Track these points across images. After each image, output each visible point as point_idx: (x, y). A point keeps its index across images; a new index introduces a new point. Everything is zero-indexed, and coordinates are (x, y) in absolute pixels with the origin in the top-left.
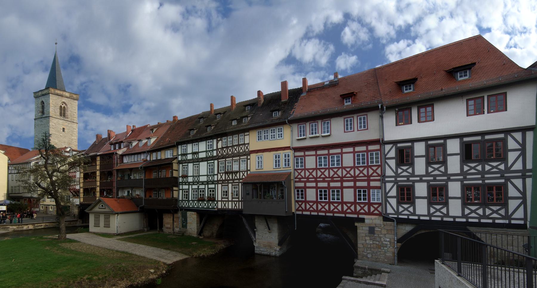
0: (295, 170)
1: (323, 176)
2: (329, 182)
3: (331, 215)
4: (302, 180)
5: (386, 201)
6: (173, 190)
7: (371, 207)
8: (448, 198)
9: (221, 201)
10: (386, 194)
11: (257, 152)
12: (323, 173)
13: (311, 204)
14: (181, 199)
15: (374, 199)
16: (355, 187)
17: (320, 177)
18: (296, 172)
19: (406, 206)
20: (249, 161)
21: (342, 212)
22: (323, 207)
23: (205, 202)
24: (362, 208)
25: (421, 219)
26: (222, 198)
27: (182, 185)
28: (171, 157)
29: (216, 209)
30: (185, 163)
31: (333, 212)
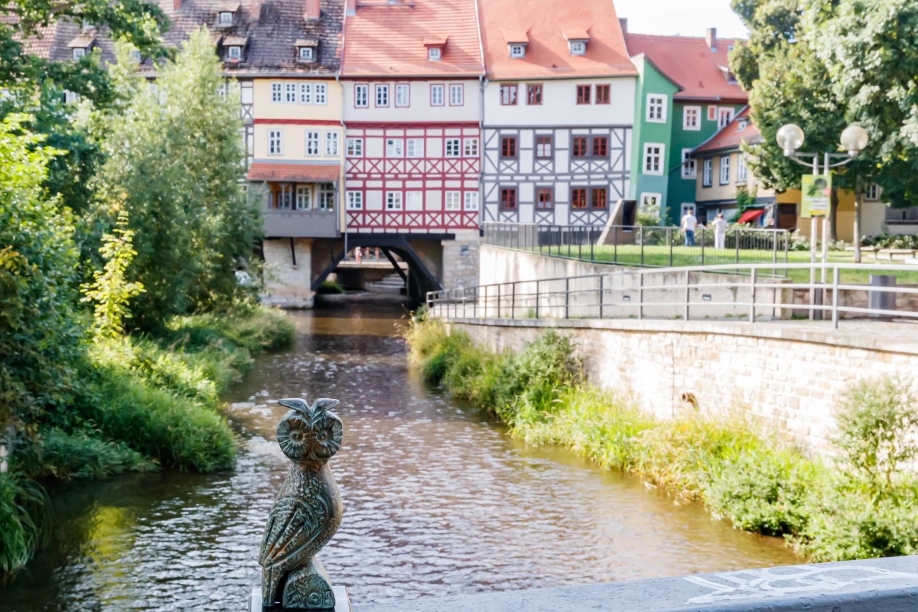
1: (395, 171)
2: (404, 180)
3: (406, 231)
4: (359, 176)
5: (484, 208)
8: (554, 203)
10: (484, 198)
12: (394, 166)
13: (374, 215)
15: (468, 206)
17: (389, 173)
18: (348, 162)
20: (250, 137)
21: (424, 226)
22: (394, 220)
31: (409, 227)
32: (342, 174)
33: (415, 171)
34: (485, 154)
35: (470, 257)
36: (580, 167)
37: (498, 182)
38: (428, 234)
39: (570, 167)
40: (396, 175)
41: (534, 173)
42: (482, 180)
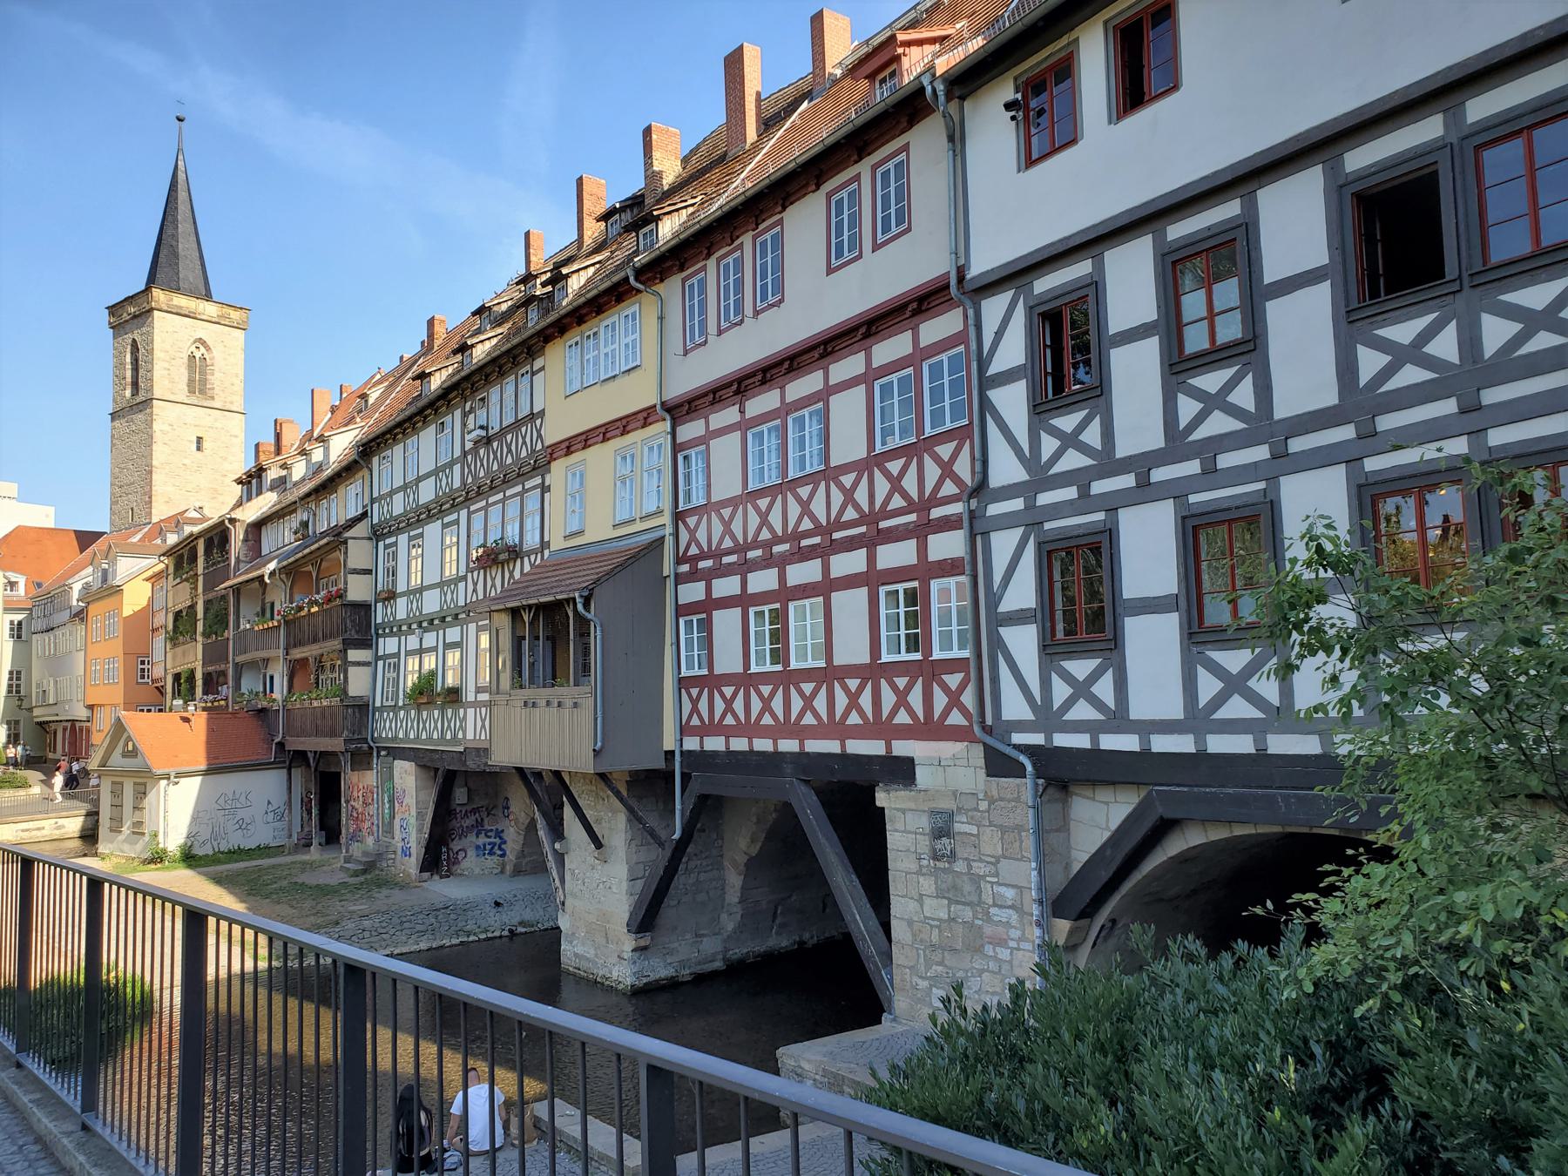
0: (678, 517)
1: (765, 535)
4: (702, 564)
5: (998, 644)
6: (346, 664)
7: (937, 690)
9: (476, 704)
10: (994, 599)
11: (568, 448)
13: (728, 691)
14: (378, 704)
16: (871, 579)
19: (1080, 668)
20: (547, 495)
23: (436, 712)
24: (902, 701)
25: (1155, 749)
26: (478, 690)
27: (385, 636)
28: (360, 511)
29: (461, 749)
30: (390, 534)
32: (668, 568)
33: (807, 524)
34: (986, 405)
35: (960, 866)
36: (1414, 353)
37: (1031, 520)
38: (844, 757)
39: (1347, 368)
40: (768, 545)
41: (1177, 443)
42: (978, 529)
